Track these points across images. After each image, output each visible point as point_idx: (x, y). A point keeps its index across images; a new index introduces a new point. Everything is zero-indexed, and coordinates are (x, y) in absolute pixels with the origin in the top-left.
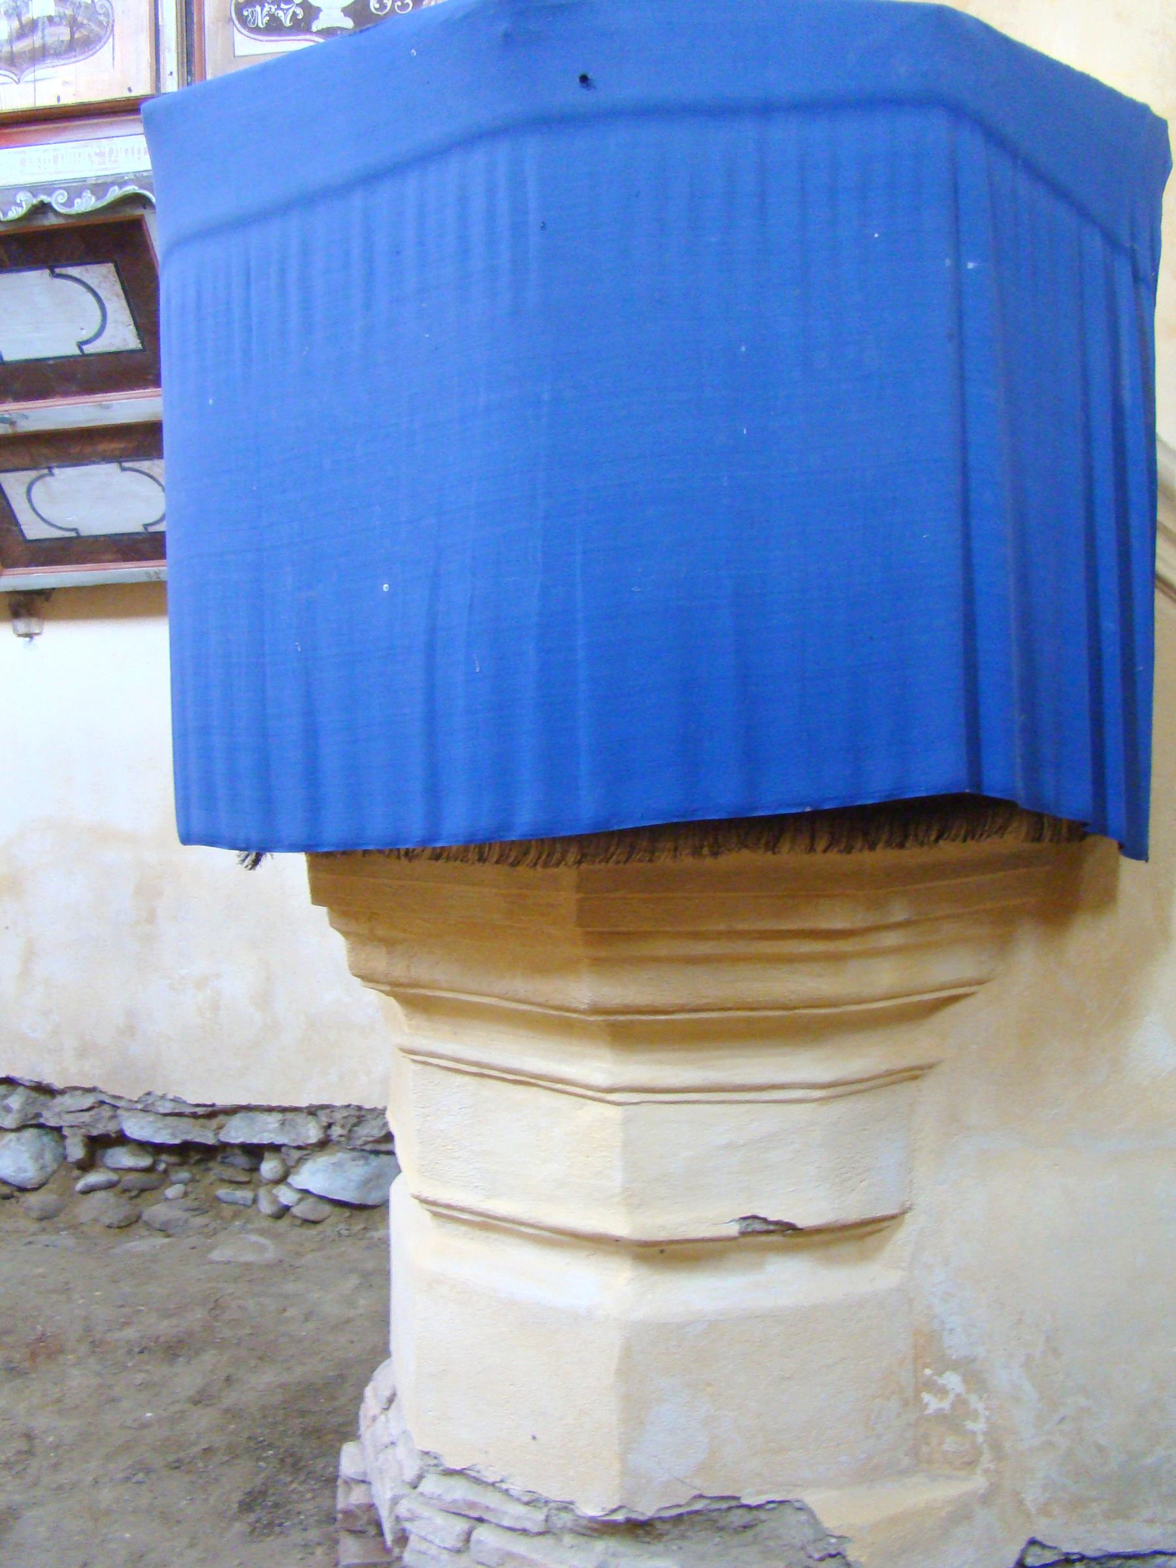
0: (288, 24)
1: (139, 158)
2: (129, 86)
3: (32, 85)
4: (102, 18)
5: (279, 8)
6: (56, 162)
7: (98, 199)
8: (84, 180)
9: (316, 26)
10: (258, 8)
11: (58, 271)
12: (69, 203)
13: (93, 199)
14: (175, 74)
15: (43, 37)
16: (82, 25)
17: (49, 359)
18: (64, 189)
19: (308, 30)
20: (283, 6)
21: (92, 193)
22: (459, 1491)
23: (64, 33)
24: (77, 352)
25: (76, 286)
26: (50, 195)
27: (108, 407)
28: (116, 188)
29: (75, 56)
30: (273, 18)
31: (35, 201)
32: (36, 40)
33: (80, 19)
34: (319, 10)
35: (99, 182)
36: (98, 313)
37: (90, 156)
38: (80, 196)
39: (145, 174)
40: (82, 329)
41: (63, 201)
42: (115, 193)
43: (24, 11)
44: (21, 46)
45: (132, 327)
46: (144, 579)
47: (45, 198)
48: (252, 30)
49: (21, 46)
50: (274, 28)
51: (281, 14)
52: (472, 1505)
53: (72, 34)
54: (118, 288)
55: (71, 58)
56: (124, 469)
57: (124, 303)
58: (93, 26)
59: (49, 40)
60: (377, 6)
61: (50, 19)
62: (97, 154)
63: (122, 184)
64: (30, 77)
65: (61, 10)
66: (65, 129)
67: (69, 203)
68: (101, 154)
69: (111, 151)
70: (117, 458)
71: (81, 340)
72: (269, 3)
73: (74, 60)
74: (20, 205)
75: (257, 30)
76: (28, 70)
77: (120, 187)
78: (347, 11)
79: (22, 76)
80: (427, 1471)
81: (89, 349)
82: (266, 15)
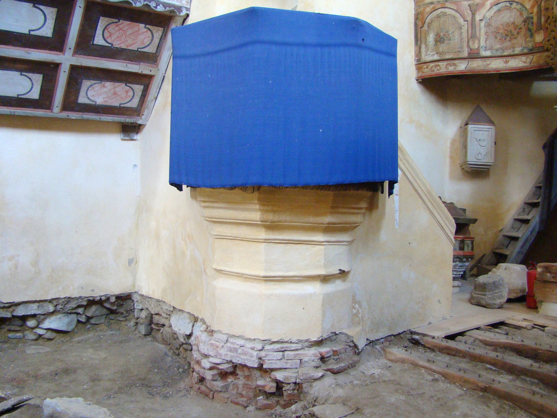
11: (36, 5)
17: (15, 32)
22: (277, 346)
24: (27, 33)
25: (41, 13)
27: (30, 53)
40: (34, 26)
45: (52, 30)
46: (8, 113)
52: (282, 348)
56: (21, 75)
57: (54, 21)
70: (21, 71)
71: (31, 29)
80: (265, 345)
81: (32, 33)
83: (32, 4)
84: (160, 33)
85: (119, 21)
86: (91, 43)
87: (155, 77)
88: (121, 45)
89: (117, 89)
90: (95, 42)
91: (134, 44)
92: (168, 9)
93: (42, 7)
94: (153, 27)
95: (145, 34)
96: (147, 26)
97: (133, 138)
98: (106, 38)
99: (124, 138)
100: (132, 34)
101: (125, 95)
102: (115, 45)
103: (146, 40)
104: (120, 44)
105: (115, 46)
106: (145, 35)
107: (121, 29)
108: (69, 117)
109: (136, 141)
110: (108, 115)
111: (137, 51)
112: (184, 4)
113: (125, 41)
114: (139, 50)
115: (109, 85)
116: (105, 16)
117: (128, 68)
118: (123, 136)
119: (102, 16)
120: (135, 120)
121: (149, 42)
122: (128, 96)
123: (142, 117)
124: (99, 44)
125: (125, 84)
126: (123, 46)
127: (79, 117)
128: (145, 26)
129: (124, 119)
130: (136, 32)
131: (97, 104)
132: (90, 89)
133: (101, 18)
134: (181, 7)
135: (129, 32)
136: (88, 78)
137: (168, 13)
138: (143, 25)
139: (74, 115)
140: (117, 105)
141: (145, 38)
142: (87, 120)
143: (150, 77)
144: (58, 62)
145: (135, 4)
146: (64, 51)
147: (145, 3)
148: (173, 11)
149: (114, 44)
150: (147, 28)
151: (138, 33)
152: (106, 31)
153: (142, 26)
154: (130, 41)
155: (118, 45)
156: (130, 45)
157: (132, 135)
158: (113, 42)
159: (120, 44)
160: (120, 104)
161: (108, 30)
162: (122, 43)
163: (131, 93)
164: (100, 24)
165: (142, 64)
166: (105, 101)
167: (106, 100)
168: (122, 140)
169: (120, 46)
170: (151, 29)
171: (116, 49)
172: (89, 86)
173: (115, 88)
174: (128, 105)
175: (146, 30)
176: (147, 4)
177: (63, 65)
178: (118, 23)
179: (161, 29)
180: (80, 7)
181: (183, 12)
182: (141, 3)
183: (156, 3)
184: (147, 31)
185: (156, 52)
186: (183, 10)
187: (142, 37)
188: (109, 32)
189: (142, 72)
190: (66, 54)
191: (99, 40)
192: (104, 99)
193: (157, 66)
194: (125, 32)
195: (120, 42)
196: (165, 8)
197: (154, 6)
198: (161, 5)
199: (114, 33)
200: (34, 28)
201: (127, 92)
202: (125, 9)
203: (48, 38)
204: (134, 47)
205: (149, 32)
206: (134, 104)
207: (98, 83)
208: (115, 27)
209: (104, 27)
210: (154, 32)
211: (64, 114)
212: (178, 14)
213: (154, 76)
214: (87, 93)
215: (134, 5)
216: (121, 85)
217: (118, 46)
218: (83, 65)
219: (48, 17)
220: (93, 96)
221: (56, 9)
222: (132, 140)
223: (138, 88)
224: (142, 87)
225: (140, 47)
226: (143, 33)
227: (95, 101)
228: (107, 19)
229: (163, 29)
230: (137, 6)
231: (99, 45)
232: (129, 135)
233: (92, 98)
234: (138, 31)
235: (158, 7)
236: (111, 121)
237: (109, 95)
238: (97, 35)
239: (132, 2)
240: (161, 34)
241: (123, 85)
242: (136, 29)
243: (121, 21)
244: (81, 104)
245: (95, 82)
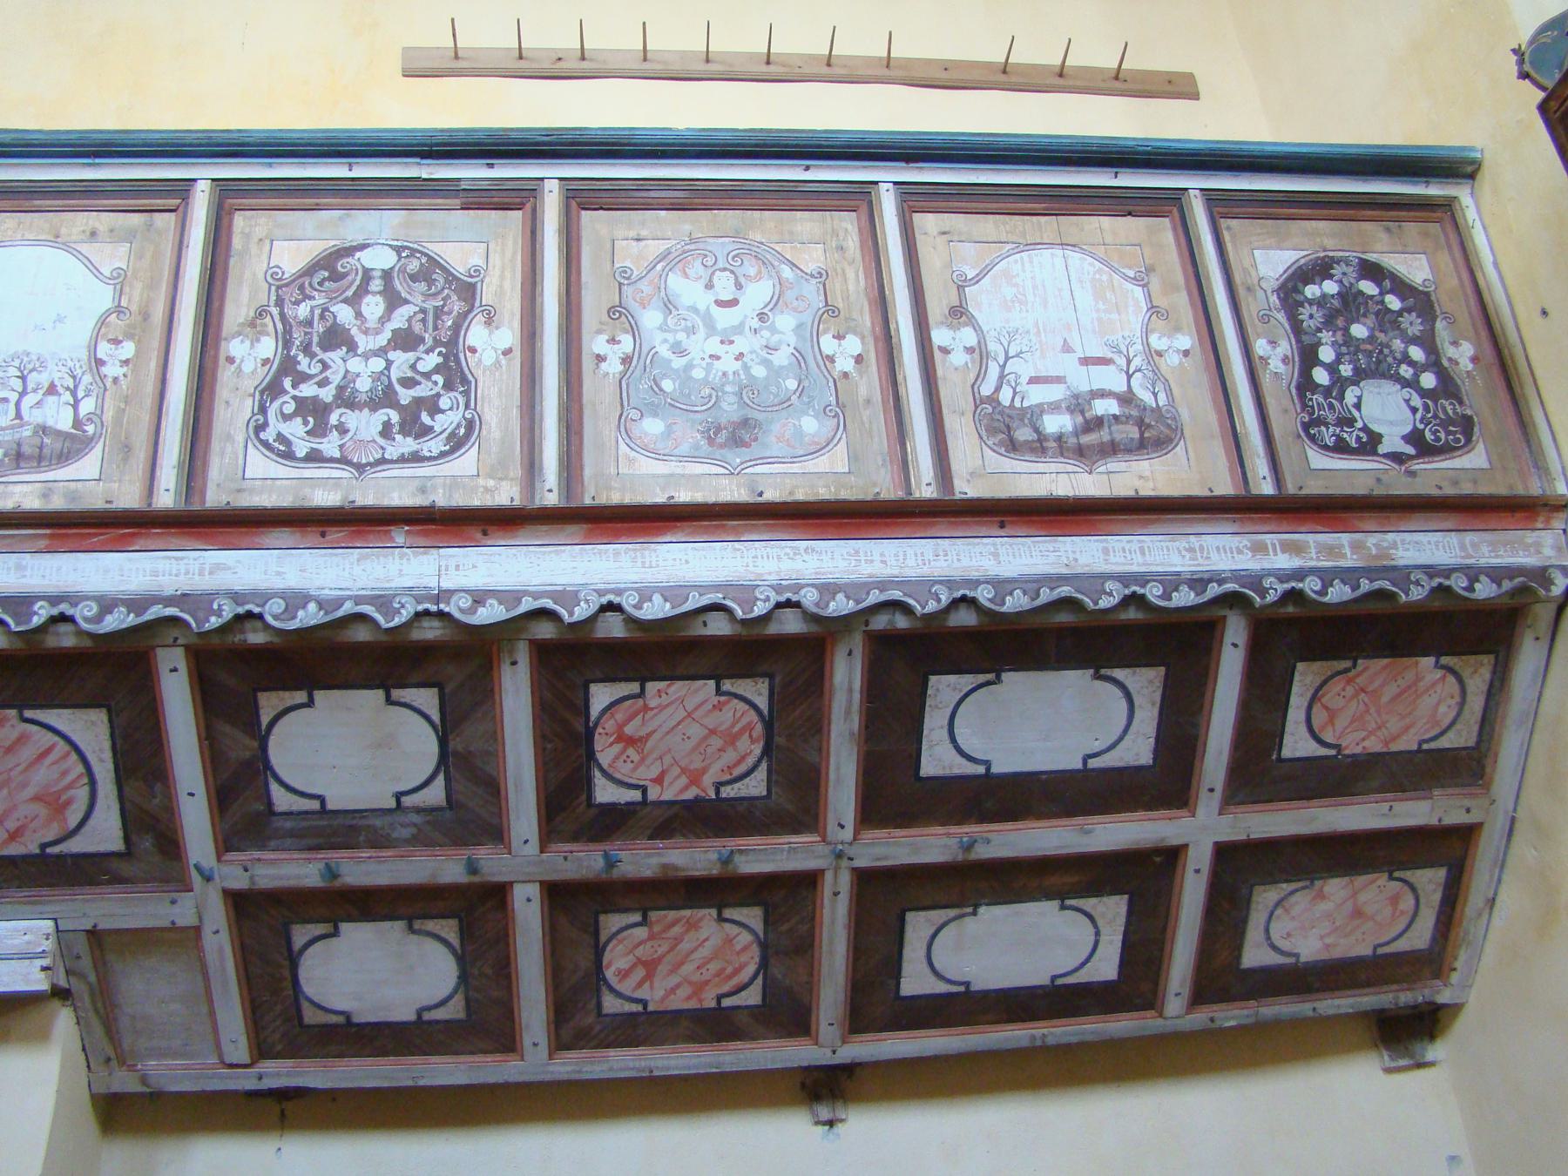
0: (1354, 445)
1: (1233, 557)
2: (1210, 486)
3: (1105, 476)
4: (1170, 422)
5: (1342, 431)
6: (1143, 553)
7: (1197, 594)
8: (1178, 574)
9: (1382, 449)
10: (1323, 428)
11: (1103, 671)
12: (1167, 596)
13: (1192, 594)
14: (1269, 479)
15: (1111, 433)
16: (1149, 426)
18: (1160, 582)
19: (1374, 452)
20: (1345, 429)
21: (1191, 588)
23: (1134, 433)
24: (1080, 766)
26: (1143, 586)
27: (1088, 832)
28: (1215, 584)
29: (1148, 454)
30: (1340, 439)
31: (1127, 592)
32: (1104, 435)
33: (1147, 420)
34: (1380, 436)
35: (1194, 577)
36: (1124, 722)
37: (1180, 552)
38: (1176, 590)
39: (1242, 573)
41: (1159, 593)
42: (1214, 590)
43: (1087, 407)
44: (1086, 439)
45: (1152, 740)
46: (1025, 1043)
47: (1140, 591)
48: (1321, 447)
49: (1086, 439)
50: (1341, 448)
51: (1345, 435)
53: (1142, 434)
54: (1158, 697)
55: (1143, 454)
56: (1063, 907)
57: (1156, 711)
58: (1162, 428)
59: (1118, 437)
60: (1433, 437)
61: (1115, 417)
62: (1186, 550)
63: (1221, 582)
64: (1102, 469)
65: (1126, 411)
66: (1153, 522)
67: (1167, 596)
68: (1191, 550)
69: (1201, 546)
70: (1060, 895)
72: (1333, 425)
73: (1147, 457)
74: (1110, 594)
75: (1326, 447)
76: (1100, 463)
77: (1220, 585)
78: (1407, 439)
79: (1094, 467)
81: (1093, 763)
82: (1332, 436)
83: (1091, 671)
84: (1485, 673)
85: (1354, 666)
86: (1274, 757)
87: (1486, 828)
88: (1366, 743)
89: (1363, 897)
90: (1287, 753)
91: (1407, 729)
92: (1507, 585)
93: (1119, 674)
94: (1463, 657)
95: (1439, 688)
96: (1444, 660)
97: (1424, 1056)
98: (1316, 730)
99: (1394, 1064)
100: (1394, 699)
101: (1388, 911)
102: (1346, 747)
103: (1443, 709)
104: (1363, 739)
105: (1347, 752)
106: (1439, 691)
107: (1363, 690)
108: (1218, 1024)
109: (1433, 1068)
110: (1337, 993)
111: (1419, 751)
112: (1550, 558)
113: (1379, 728)
114: (1425, 746)
115: (1336, 887)
116: (1311, 655)
117: (1395, 816)
118: (1390, 1056)
119: (1303, 660)
120: (1427, 992)
121: (1452, 714)
122: (1397, 914)
123: (1448, 977)
124: (1298, 754)
125: (1386, 875)
126: (1374, 745)
127: (1247, 1016)
128: (1437, 662)
129: (1391, 996)
130: (1409, 687)
131: (1302, 959)
132: (1276, 913)
133: (1300, 666)
134: (1544, 569)
135: (1391, 690)
136: (1271, 880)
137: (1506, 600)
138: (1430, 661)
139: (1230, 1016)
140: (1364, 950)
141: (1438, 704)
142: (1276, 1024)
143: (1466, 834)
144: (1175, 842)
145: (1407, 594)
146: (1191, 801)
147: (1436, 581)
148: (1523, 590)
149: (1344, 745)
150: (1443, 667)
151: (1416, 690)
152: (1316, 708)
153: (1428, 661)
154: (1394, 725)
155: (1358, 744)
156: (1394, 739)
157: (1417, 1047)
158: (1340, 738)
159: (1363, 739)
160: (1375, 948)
161: (1324, 700)
162: (1371, 733)
163: (1407, 902)
164: (1295, 689)
165: (1436, 793)
166: (1327, 946)
167: (1328, 941)
168: (1388, 1070)
169: (1364, 748)
170: (1457, 668)
171: (1350, 760)
172: (1271, 904)
173: (1355, 894)
174: (1402, 945)
175: (1439, 674)
176: (1440, 584)
177: (1191, 852)
178: (1353, 673)
179: (1487, 660)
180: (1235, 645)
181: (1556, 581)
182: (1423, 586)
183: (1466, 575)
184: (1444, 677)
185: (1479, 742)
186: (1553, 576)
187: (1428, 701)
188: (1326, 708)
189: (1440, 820)
190: (1201, 811)
191: (1296, 742)
192: (1322, 938)
193: (1487, 787)
194: (1375, 695)
195: (1364, 734)
196: (1499, 585)
197: (1463, 585)
198: (1483, 578)
199: (1343, 708)
200: (1097, 746)
201: (1395, 900)
202: (1372, 619)
203: (1139, 769)
204: (1407, 743)
205: (1451, 679)
206: (1420, 937)
207: (1303, 888)
208: (1341, 686)
209: (1309, 695)
210: (1465, 674)
211: (1199, 1018)
212: (1544, 593)
213: (1479, 826)
214: (1267, 930)
215: (1404, 597)
216: (1374, 881)
217: (1358, 750)
218: (1251, 837)
219: (1137, 701)
220: (1289, 935)
221: (1162, 670)
222: (1420, 1065)
223: (1431, 880)
224: (1441, 874)
225: (1427, 736)
226: (1434, 685)
227: (1296, 951)
228: (1317, 665)
229: (1492, 657)
230: (1415, 598)
231: (1299, 759)
232: (1407, 1048)
233: (1284, 945)
234: (1415, 683)
235: (1477, 586)
236: (1351, 1011)
237: (1338, 924)
238: (1290, 726)
239: (1394, 589)
240: (1488, 676)
241: (1382, 879)
242: (1410, 676)
243: (1360, 661)
244: (1252, 971)
245: (1294, 886)
